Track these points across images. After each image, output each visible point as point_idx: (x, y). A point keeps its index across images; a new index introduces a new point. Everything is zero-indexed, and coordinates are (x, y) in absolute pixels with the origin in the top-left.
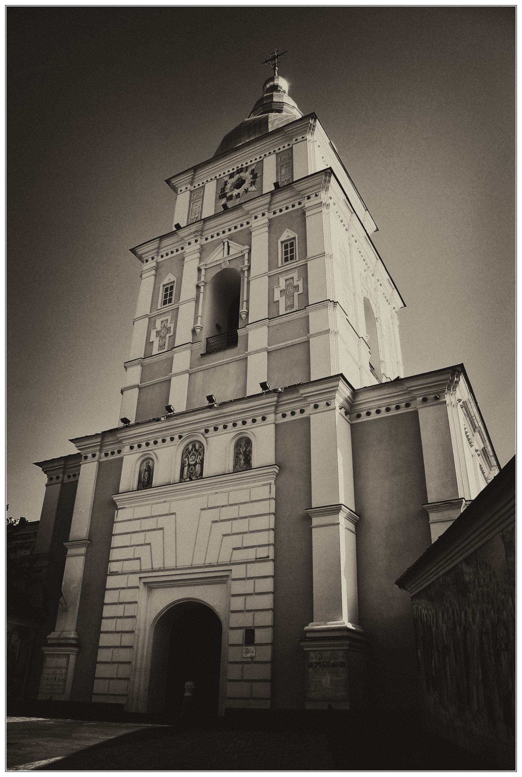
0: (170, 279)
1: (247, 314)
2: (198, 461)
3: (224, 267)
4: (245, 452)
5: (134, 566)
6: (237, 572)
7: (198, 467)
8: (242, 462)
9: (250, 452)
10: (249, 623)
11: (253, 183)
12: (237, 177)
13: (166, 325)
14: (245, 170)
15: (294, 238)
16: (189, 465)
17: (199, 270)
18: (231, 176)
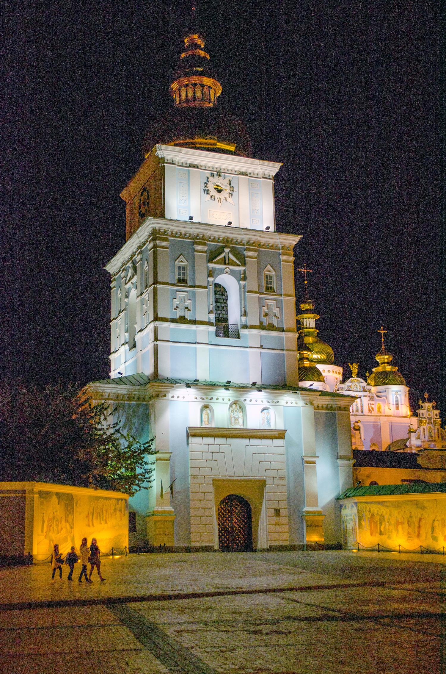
10: (277, 507)
16: (235, 418)
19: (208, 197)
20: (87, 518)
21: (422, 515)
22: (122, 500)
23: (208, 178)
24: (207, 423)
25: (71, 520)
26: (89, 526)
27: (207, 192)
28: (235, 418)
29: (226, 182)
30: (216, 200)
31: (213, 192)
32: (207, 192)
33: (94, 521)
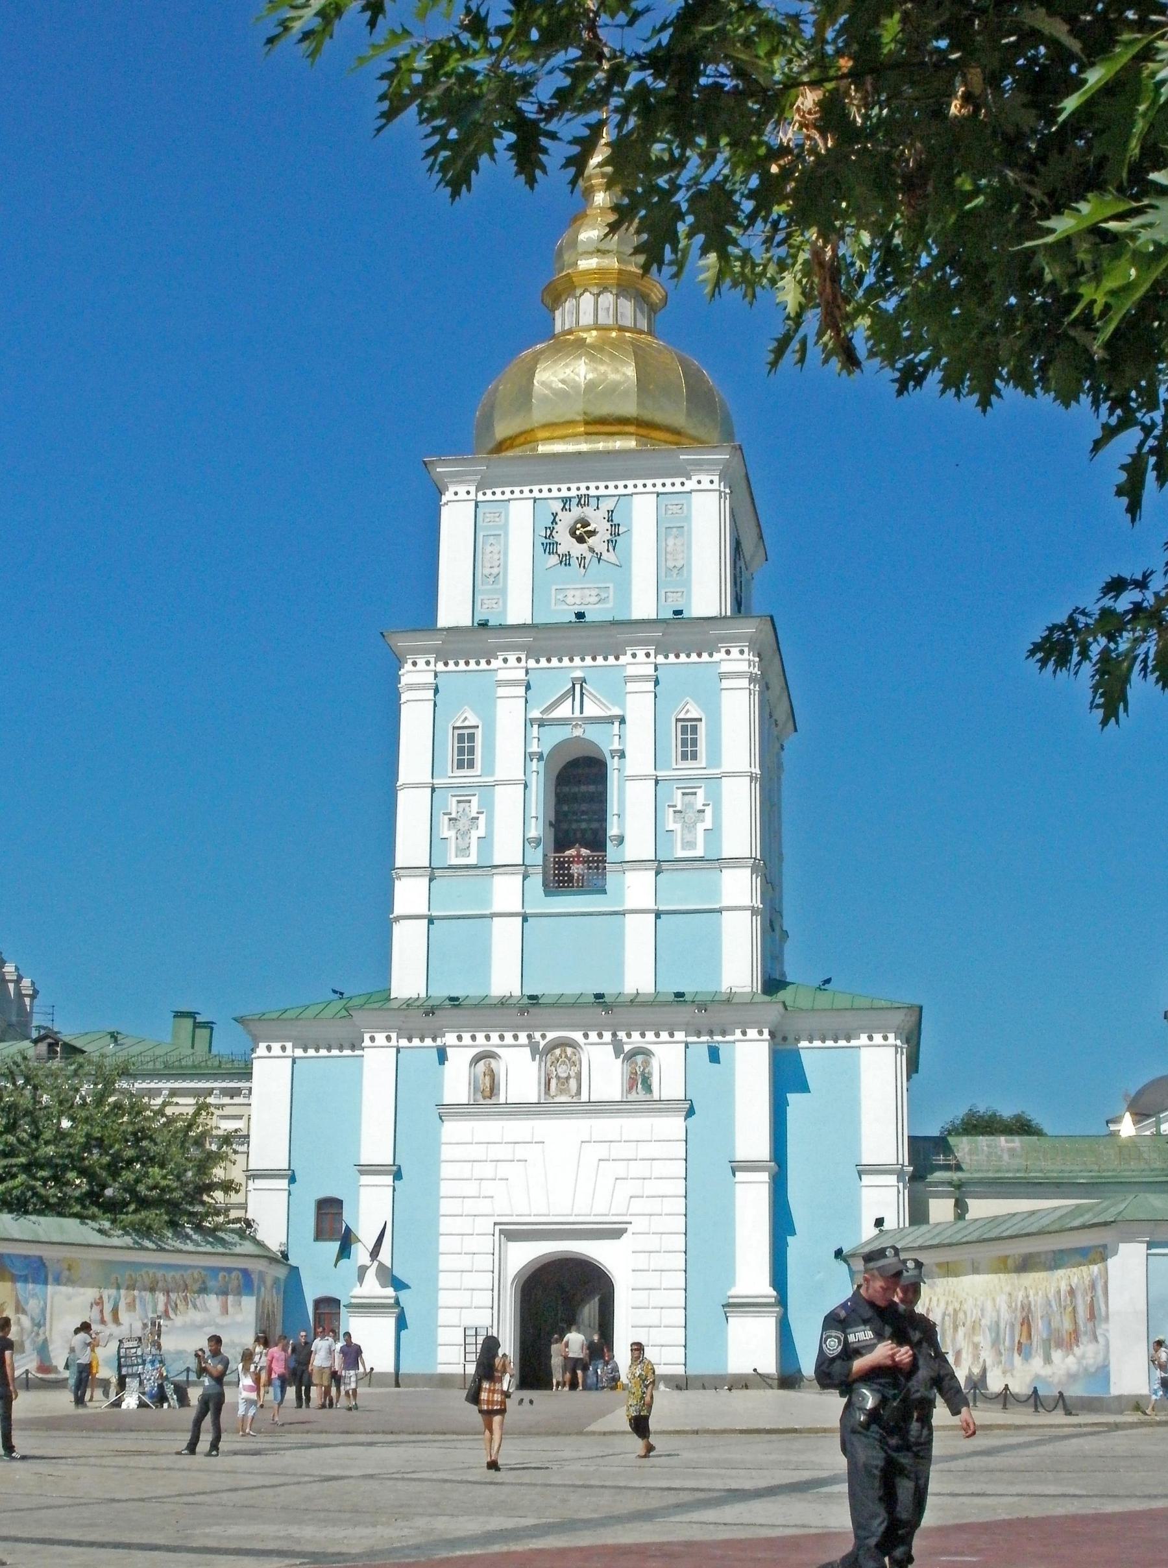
0: (466, 719)
1: (621, 840)
2: (572, 1074)
3: (578, 732)
4: (643, 1074)
5: (483, 1206)
6: (638, 1224)
7: (573, 1083)
8: (640, 1086)
9: (650, 1073)
11: (612, 543)
12: (576, 512)
13: (467, 809)
14: (593, 501)
15: (700, 720)
16: (558, 1077)
17: (529, 722)
18: (566, 501)
19: (554, 559)
20: (96, 1309)
21: (930, 1300)
22: (229, 1270)
23: (555, 515)
24: (488, 1094)
25: (37, 1311)
26: (103, 1322)
27: (550, 546)
28: (558, 1077)
29: (603, 512)
30: (574, 562)
31: (567, 544)
32: (550, 546)
33: (124, 1316)
